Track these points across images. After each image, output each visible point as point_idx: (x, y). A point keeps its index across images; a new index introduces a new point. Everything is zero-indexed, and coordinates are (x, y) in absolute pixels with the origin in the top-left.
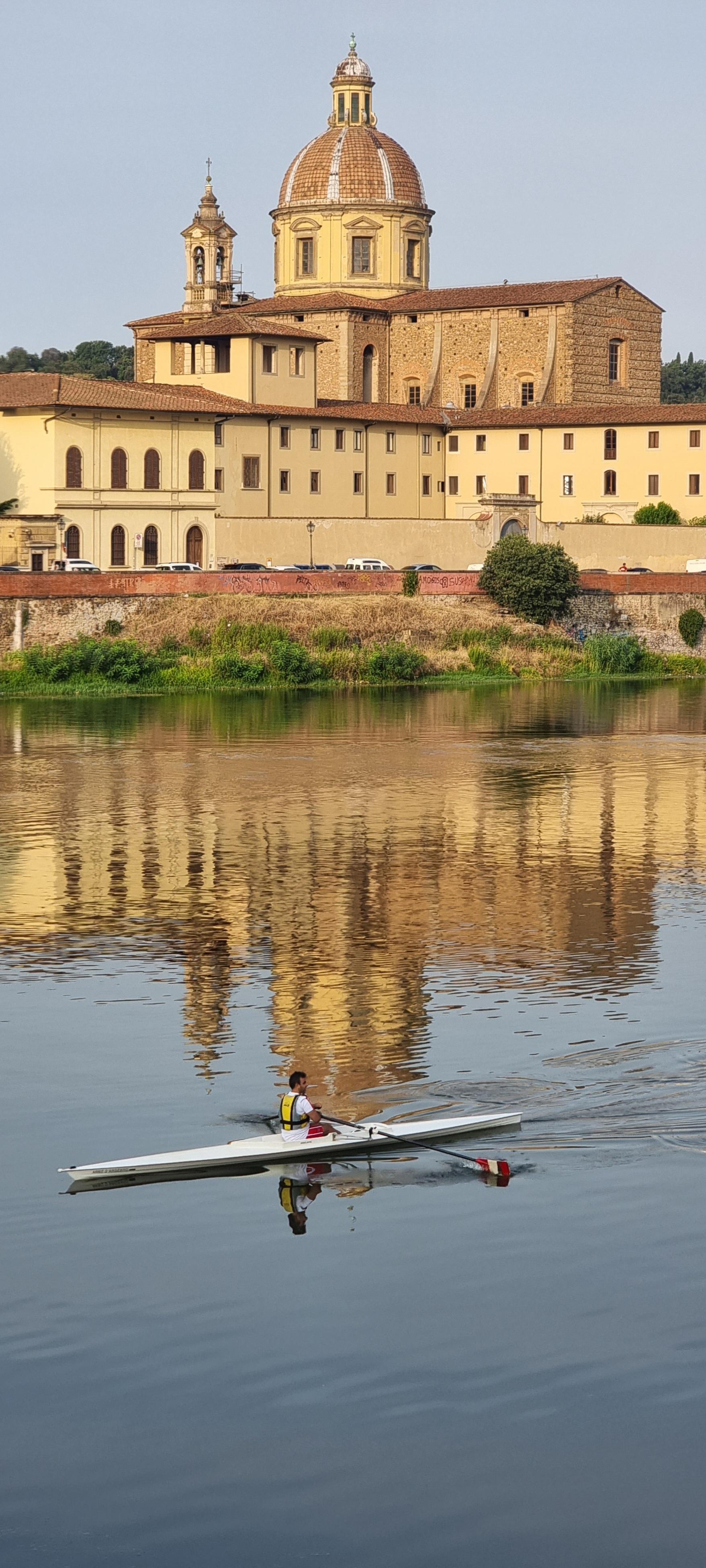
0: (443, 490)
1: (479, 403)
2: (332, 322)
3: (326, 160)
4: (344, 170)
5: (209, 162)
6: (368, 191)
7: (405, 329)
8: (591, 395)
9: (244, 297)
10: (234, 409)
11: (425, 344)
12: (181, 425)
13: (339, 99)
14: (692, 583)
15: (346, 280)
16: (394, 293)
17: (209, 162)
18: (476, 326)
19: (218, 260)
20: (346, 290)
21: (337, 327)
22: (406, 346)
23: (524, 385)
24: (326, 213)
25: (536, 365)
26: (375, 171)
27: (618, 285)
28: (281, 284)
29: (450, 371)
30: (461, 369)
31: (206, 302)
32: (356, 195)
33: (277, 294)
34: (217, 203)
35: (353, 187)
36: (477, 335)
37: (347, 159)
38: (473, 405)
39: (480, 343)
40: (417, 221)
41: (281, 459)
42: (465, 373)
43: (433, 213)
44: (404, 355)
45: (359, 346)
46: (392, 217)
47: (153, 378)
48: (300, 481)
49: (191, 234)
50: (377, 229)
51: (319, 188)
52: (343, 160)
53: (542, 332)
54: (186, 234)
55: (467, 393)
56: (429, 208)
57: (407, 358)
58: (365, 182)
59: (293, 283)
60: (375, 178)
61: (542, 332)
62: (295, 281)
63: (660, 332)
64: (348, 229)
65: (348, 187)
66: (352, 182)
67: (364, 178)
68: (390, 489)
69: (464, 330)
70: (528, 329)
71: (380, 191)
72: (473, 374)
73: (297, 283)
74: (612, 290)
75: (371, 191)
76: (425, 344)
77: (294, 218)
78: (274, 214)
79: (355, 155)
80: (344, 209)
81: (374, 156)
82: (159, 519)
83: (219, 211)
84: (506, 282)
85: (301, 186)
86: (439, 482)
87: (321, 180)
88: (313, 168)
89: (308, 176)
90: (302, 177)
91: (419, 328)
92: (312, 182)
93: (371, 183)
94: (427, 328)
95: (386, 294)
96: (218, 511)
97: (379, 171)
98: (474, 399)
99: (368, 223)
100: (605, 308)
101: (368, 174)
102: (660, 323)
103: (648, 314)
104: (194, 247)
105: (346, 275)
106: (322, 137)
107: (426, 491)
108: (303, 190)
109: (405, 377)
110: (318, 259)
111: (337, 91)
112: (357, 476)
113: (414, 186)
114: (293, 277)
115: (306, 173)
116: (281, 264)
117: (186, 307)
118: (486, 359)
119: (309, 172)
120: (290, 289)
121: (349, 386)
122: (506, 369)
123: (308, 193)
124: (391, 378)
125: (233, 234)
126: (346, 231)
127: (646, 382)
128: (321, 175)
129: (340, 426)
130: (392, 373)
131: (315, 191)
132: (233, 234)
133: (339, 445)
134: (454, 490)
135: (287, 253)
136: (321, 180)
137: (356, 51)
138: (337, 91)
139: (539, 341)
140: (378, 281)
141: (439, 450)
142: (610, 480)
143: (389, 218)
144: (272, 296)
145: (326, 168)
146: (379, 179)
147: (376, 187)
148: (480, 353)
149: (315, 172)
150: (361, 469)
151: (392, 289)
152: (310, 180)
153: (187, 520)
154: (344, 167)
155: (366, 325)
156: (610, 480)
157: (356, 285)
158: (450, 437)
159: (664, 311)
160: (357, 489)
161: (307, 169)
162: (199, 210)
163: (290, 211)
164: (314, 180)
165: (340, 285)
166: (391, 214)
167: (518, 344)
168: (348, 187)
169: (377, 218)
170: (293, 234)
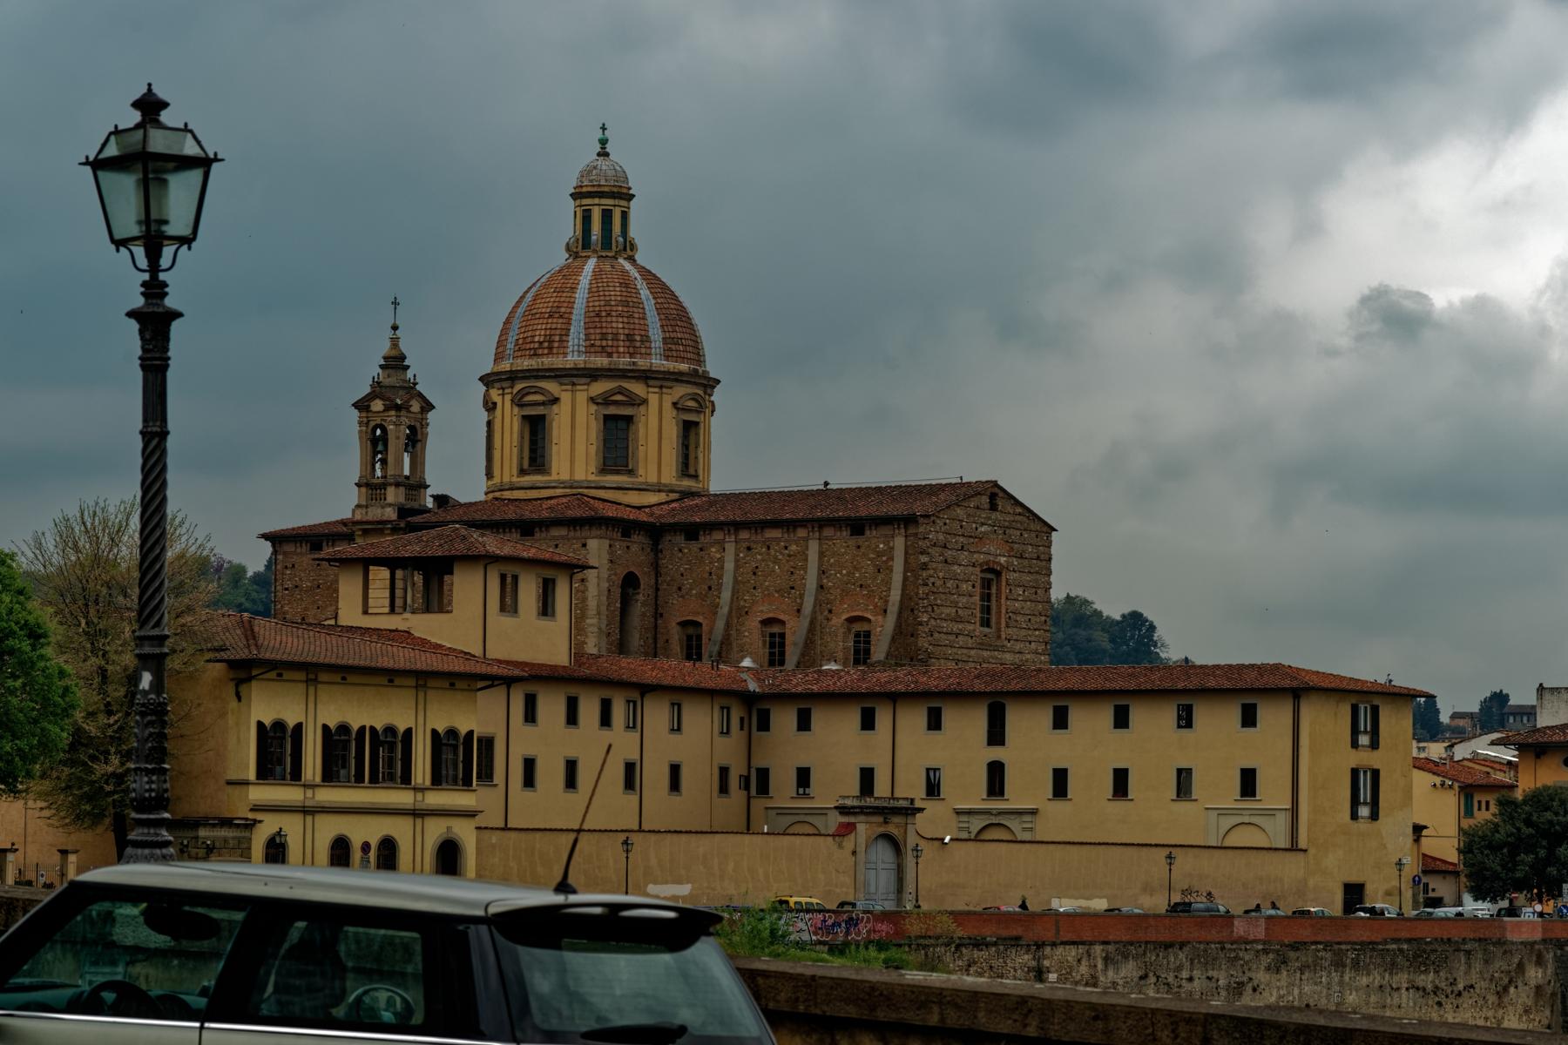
0: (747, 788)
1: (791, 658)
3: (565, 305)
4: (592, 320)
5: (395, 303)
6: (626, 350)
7: (680, 550)
8: (955, 650)
9: (442, 500)
10: (517, 672)
11: (710, 574)
12: (431, 693)
13: (584, 218)
14: (1147, 928)
15: (592, 478)
16: (662, 497)
17: (395, 303)
18: (786, 548)
19: (407, 445)
20: (593, 493)
22: (682, 575)
23: (857, 635)
24: (566, 380)
25: (876, 606)
26: (636, 321)
27: (994, 494)
28: (496, 480)
29: (747, 613)
30: (765, 610)
31: (390, 505)
32: (610, 355)
33: (491, 496)
34: (406, 363)
35: (604, 343)
36: (788, 561)
37: (597, 304)
38: (782, 663)
39: (792, 573)
40: (696, 394)
41: (523, 741)
42: (771, 615)
43: (718, 382)
44: (680, 589)
45: (615, 574)
46: (661, 387)
47: (336, 618)
48: (550, 774)
49: (369, 406)
50: (639, 405)
51: (556, 345)
52: (591, 304)
53: (884, 559)
54: (362, 406)
55: (772, 645)
56: (711, 375)
57: (684, 592)
58: (622, 337)
59: (515, 479)
60: (636, 332)
61: (884, 559)
62: (518, 477)
63: (1050, 559)
64: (597, 404)
65: (598, 343)
66: (604, 336)
67: (621, 331)
68: (675, 785)
69: (769, 554)
70: (863, 554)
72: (782, 617)
73: (519, 479)
74: (985, 500)
75: (631, 350)
76: (710, 574)
77: (519, 386)
78: (487, 380)
79: (608, 298)
80: (593, 375)
81: (635, 300)
82: (400, 830)
83: (410, 374)
84: (826, 484)
85: (529, 340)
86: (740, 776)
87: (558, 332)
88: (547, 315)
89: (539, 327)
90: (531, 328)
91: (701, 550)
93: (630, 338)
94: (713, 550)
95: (653, 498)
96: (480, 821)
97: (642, 322)
98: (782, 654)
99: (627, 396)
100: (974, 526)
101: (626, 326)
102: (1049, 547)
103: (1033, 535)
104: (372, 424)
106: (560, 271)
107: (724, 789)
108: (532, 346)
109: (679, 620)
110: (554, 447)
111: (581, 206)
112: (630, 768)
113: (690, 343)
114: (515, 471)
115: (536, 322)
116: (497, 454)
117: (358, 512)
118: (802, 596)
119: (541, 321)
120: (511, 489)
122: (830, 611)
123: (540, 352)
124: (659, 622)
125: (428, 406)
126: (593, 408)
127: (1030, 632)
129: (573, 690)
131: (550, 348)
132: (428, 406)
133: (572, 719)
134: (764, 789)
135: (507, 435)
136: (558, 332)
137: (607, 150)
138: (581, 206)
139: (879, 571)
140: (641, 479)
141: (742, 729)
142: (996, 772)
143: (656, 390)
144: (482, 497)
145: (566, 316)
146: (643, 333)
147: (638, 344)
148: (792, 588)
149: (550, 321)
150: (635, 756)
151: (659, 491)
152: (543, 332)
153: (435, 830)
154: (592, 314)
155: (625, 544)
156: (996, 772)
157: (607, 485)
158: (759, 710)
159: (1056, 530)
160: (629, 784)
161: (538, 316)
162: (380, 371)
163: (513, 376)
164: (548, 333)
166: (658, 383)
167: (848, 574)
168: (598, 343)
169: (638, 388)
170: (516, 410)
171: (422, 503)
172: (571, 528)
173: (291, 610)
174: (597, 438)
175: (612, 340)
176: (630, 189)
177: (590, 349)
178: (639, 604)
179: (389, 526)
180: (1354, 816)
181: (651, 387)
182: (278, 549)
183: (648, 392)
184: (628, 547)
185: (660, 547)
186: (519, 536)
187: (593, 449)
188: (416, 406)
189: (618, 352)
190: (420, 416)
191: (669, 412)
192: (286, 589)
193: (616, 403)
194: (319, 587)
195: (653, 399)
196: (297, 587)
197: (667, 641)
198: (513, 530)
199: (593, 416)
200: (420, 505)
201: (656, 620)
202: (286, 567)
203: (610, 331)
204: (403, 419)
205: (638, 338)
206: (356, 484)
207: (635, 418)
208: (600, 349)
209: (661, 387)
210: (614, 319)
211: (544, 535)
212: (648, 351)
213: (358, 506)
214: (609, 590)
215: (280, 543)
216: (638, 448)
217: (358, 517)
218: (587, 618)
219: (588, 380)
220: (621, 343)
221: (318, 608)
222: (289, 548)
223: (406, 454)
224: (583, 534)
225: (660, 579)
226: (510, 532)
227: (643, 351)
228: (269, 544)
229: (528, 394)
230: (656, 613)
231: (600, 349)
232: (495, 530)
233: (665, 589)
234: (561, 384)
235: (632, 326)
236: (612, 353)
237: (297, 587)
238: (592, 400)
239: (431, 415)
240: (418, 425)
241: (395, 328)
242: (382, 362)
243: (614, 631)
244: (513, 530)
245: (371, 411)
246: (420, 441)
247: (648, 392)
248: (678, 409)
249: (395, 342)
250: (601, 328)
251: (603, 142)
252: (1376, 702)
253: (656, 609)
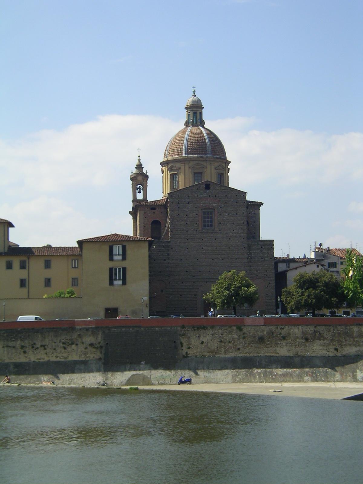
32: (172, 156)
143: (183, 164)
146: (181, 148)
176: (202, 105)
180: (111, 283)
209: (184, 163)
212: (182, 153)
219: (166, 165)
231: (170, 155)
241: (139, 157)
242: (136, 167)
249: (139, 160)
251: (194, 92)
252: (124, 244)
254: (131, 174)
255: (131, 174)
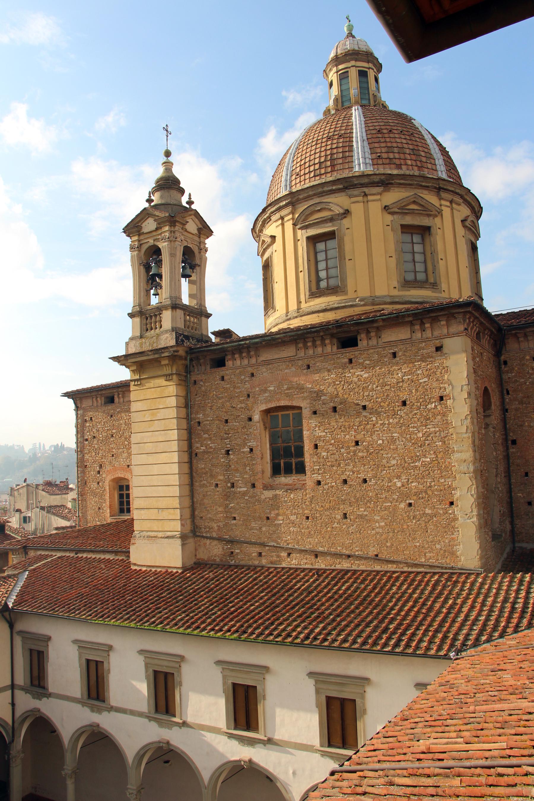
2: (427, 340)
4: (375, 136)
6: (414, 163)
9: (225, 334)
15: (396, 293)
21: (439, 349)
24: (356, 192)
31: (166, 331)
32: (399, 167)
35: (391, 156)
58: (408, 151)
60: (420, 149)
66: (390, 150)
67: (405, 146)
71: (429, 166)
75: (419, 164)
77: (301, 208)
92: (326, 156)
93: (415, 152)
101: (410, 142)
105: (395, 284)
117: (132, 344)
121: (475, 471)
128: (341, 145)
130: (514, 442)
146: (426, 150)
147: (424, 159)
165: (388, 300)
166: (449, 196)
168: (385, 156)
171: (204, 333)
172: (417, 327)
173: (90, 458)
174: (396, 250)
175: (399, 153)
177: (377, 159)
178: (492, 430)
179: (166, 354)
181: (443, 199)
182: (79, 405)
183: (441, 205)
184: (481, 353)
185: (502, 358)
186: (335, 348)
187: (393, 262)
188: (192, 226)
189: (406, 164)
190: (197, 239)
191: (461, 231)
192: (87, 440)
193: (412, 212)
194: (112, 436)
195: (446, 212)
196: (94, 437)
197: (527, 474)
198: (327, 341)
199: (390, 227)
200: (202, 334)
201: (507, 449)
202: (86, 421)
203: (395, 145)
204: (177, 234)
205: (423, 154)
206: (128, 314)
207: (432, 229)
208: (387, 161)
209: (451, 202)
210: (397, 136)
211: (373, 342)
213: (131, 339)
214: (477, 410)
215: (81, 399)
216: (438, 262)
217: (132, 351)
218: (454, 452)
220: (408, 157)
221: (113, 455)
222: (87, 403)
223: (183, 280)
224: (436, 333)
225: (507, 398)
226: (324, 345)
227: (429, 166)
228: (71, 401)
229: (312, 213)
230: (506, 440)
232: (301, 345)
233: (516, 410)
234: (350, 197)
235: (415, 143)
236: (401, 165)
237: (94, 437)
238: (386, 208)
239: (209, 242)
240: (196, 250)
241: (168, 154)
243: (484, 469)
244: (327, 341)
245: (143, 233)
246: (199, 266)
247: (441, 205)
248: (464, 226)
249: (168, 166)
250: (386, 142)
253: (506, 435)
254: (147, 205)
255: (147, 205)
